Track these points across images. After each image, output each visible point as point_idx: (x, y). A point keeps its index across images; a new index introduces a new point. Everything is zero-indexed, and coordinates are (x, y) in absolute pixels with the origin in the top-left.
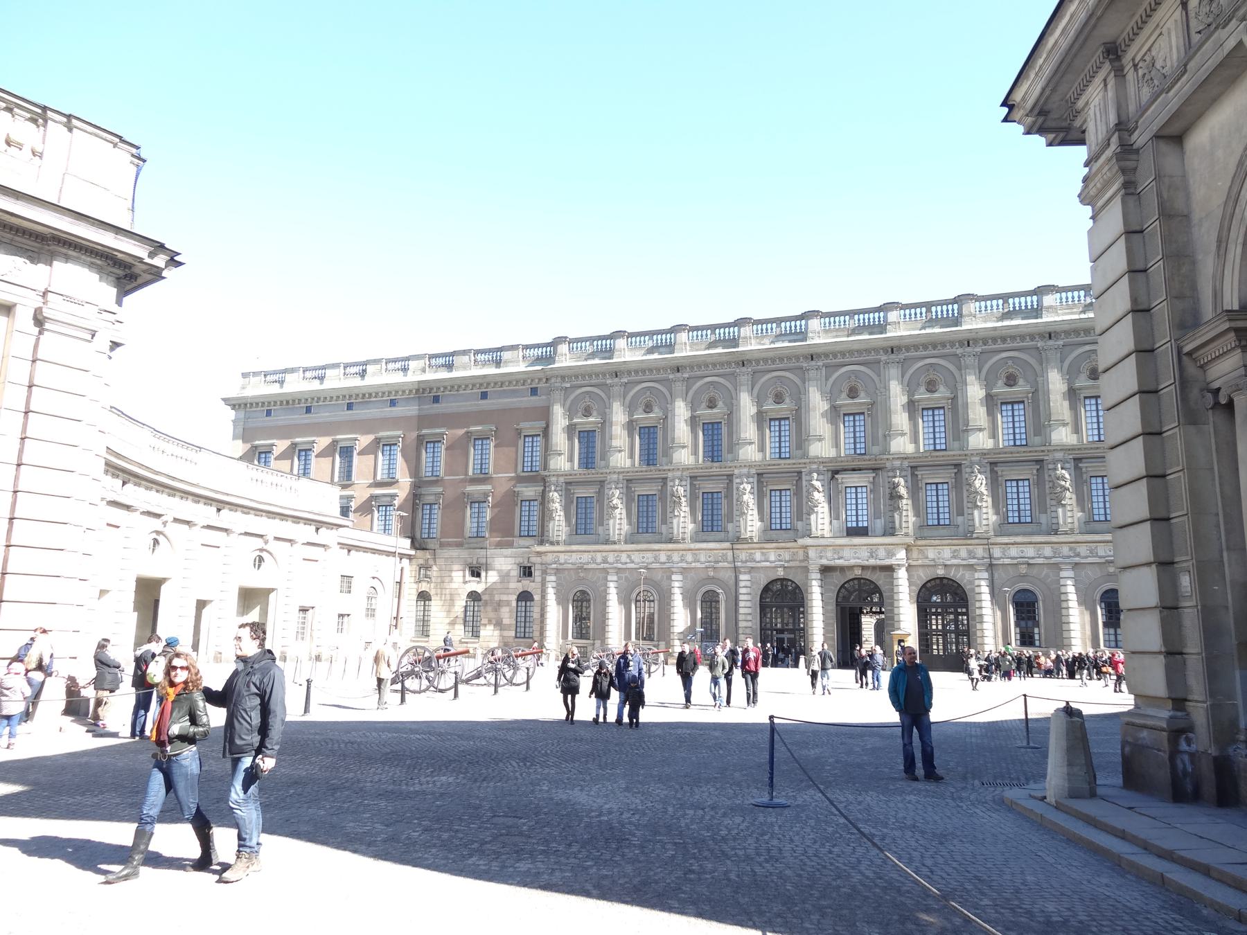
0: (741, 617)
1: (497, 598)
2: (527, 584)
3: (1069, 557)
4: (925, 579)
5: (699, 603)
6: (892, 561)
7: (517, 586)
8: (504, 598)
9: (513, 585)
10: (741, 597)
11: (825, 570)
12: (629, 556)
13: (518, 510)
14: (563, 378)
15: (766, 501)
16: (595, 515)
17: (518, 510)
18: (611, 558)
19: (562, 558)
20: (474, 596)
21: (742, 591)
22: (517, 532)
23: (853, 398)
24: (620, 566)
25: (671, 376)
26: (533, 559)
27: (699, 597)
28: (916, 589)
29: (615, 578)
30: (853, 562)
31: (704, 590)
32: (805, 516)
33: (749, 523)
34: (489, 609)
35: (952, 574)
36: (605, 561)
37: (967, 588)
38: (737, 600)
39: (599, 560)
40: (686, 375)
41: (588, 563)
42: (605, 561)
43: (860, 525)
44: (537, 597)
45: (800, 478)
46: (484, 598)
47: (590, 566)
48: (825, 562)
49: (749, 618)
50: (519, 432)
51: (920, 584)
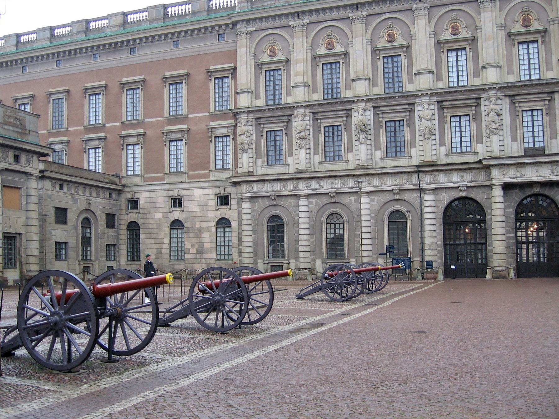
0: (426, 234)
1: (198, 225)
2: (224, 212)
5: (386, 223)
7: (215, 214)
8: (204, 224)
10: (427, 216)
11: (507, 187)
13: (212, 145)
14: (248, 21)
15: (447, 127)
16: (285, 146)
17: (212, 145)
19: (256, 187)
20: (176, 225)
21: (427, 210)
22: (212, 167)
23: (526, 26)
25: (351, 15)
26: (229, 190)
27: (386, 217)
30: (534, 179)
32: (485, 139)
34: (191, 235)
38: (422, 219)
40: (365, 13)
43: (537, 145)
44: (234, 223)
45: (478, 105)
47: (282, 193)
48: (508, 180)
49: (434, 234)
50: (210, 73)
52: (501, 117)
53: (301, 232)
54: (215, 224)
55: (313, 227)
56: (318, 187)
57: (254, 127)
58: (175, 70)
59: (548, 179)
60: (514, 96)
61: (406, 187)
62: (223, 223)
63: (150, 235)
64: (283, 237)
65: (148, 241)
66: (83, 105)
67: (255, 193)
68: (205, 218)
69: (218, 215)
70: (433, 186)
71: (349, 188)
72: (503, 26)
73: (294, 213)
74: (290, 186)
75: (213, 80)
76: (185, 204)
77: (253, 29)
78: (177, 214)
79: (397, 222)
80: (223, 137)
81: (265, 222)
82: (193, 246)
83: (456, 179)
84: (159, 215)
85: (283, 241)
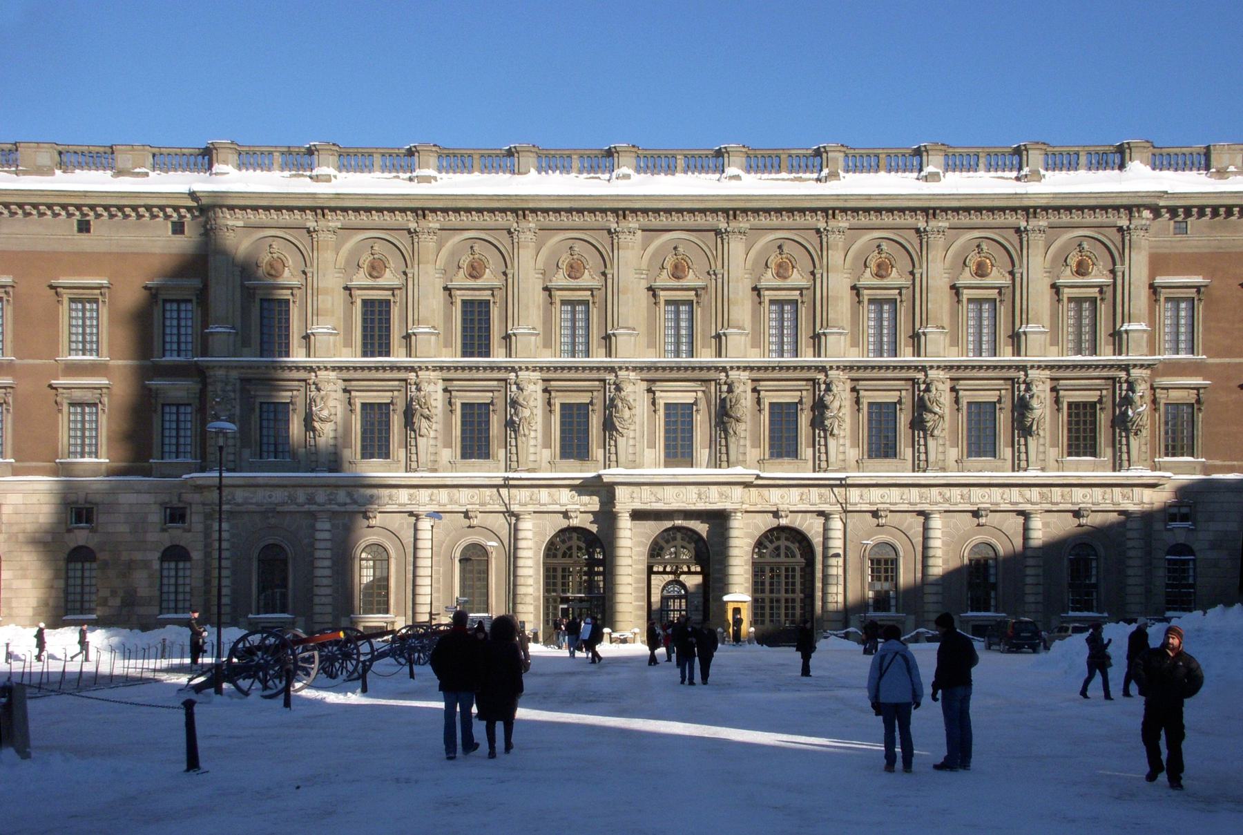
1: (125, 556)
2: (177, 535)
3: (936, 504)
4: (764, 529)
6: (728, 506)
7: (159, 538)
8: (138, 556)
9: (153, 536)
11: (637, 515)
12: (350, 495)
18: (321, 496)
23: (678, 278)
24: (336, 508)
25: (412, 225)
26: (189, 497)
28: (752, 542)
29: (327, 526)
30: (675, 506)
31: (464, 543)
33: (532, 450)
35: (798, 522)
36: (311, 500)
39: (301, 499)
41: (283, 504)
42: (311, 500)
44: (196, 555)
46: (102, 556)
47: (286, 508)
48: (638, 506)
51: (758, 534)
52: (633, 411)
53: (318, 572)
54: (158, 555)
56: (348, 501)
57: (238, 395)
58: (80, 274)
59: (693, 507)
60: (654, 381)
61: (489, 508)
64: (285, 579)
65: (17, 584)
67: (238, 505)
69: (166, 539)
71: (400, 505)
73: (306, 541)
74: (301, 495)
75: (160, 303)
76: (102, 518)
77: (241, 223)
79: (473, 561)
80: (178, 405)
81: (256, 555)
82: (114, 593)
85: (286, 586)
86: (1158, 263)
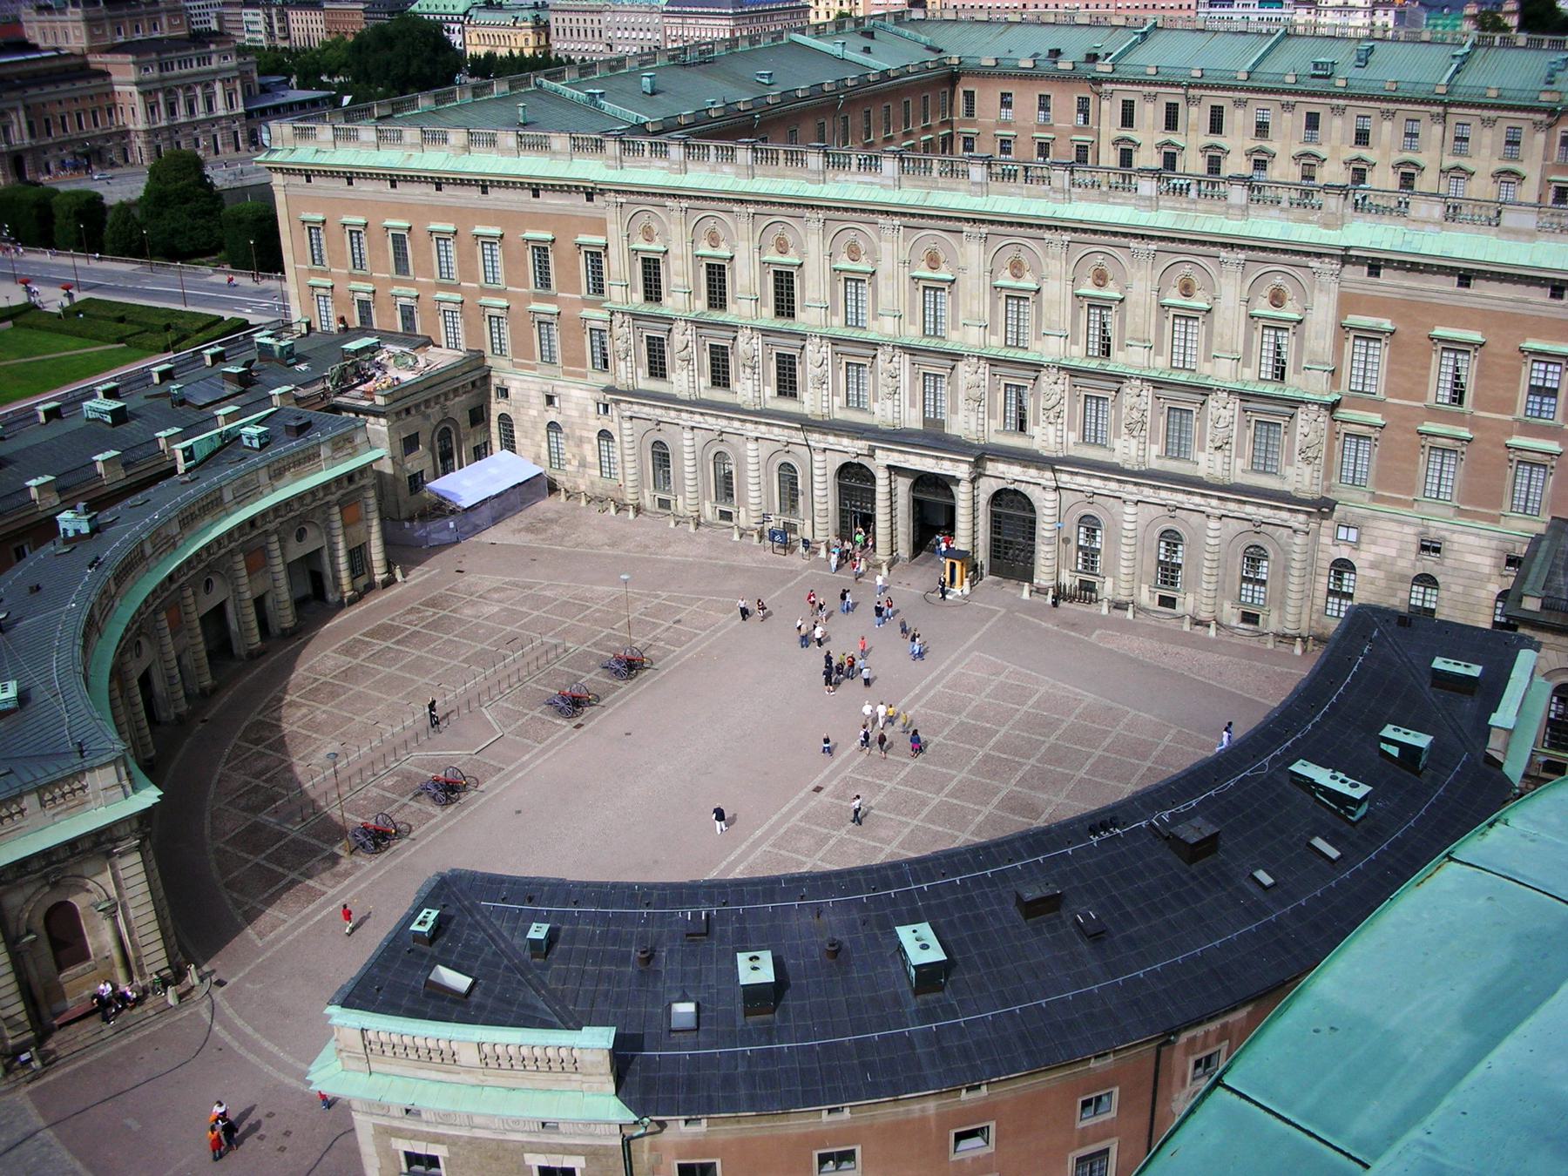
1: (578, 433)
6: (958, 475)
8: (585, 434)
14: (617, 191)
20: (553, 426)
27: (776, 468)
35: (1022, 488)
37: (1036, 505)
55: (699, 465)
62: (604, 435)
63: (526, 434)
66: (430, 249)
68: (585, 426)
69: (599, 425)
70: (823, 446)
72: (908, 263)
78: (552, 415)
83: (846, 441)
84: (533, 413)
86: (1347, 303)
